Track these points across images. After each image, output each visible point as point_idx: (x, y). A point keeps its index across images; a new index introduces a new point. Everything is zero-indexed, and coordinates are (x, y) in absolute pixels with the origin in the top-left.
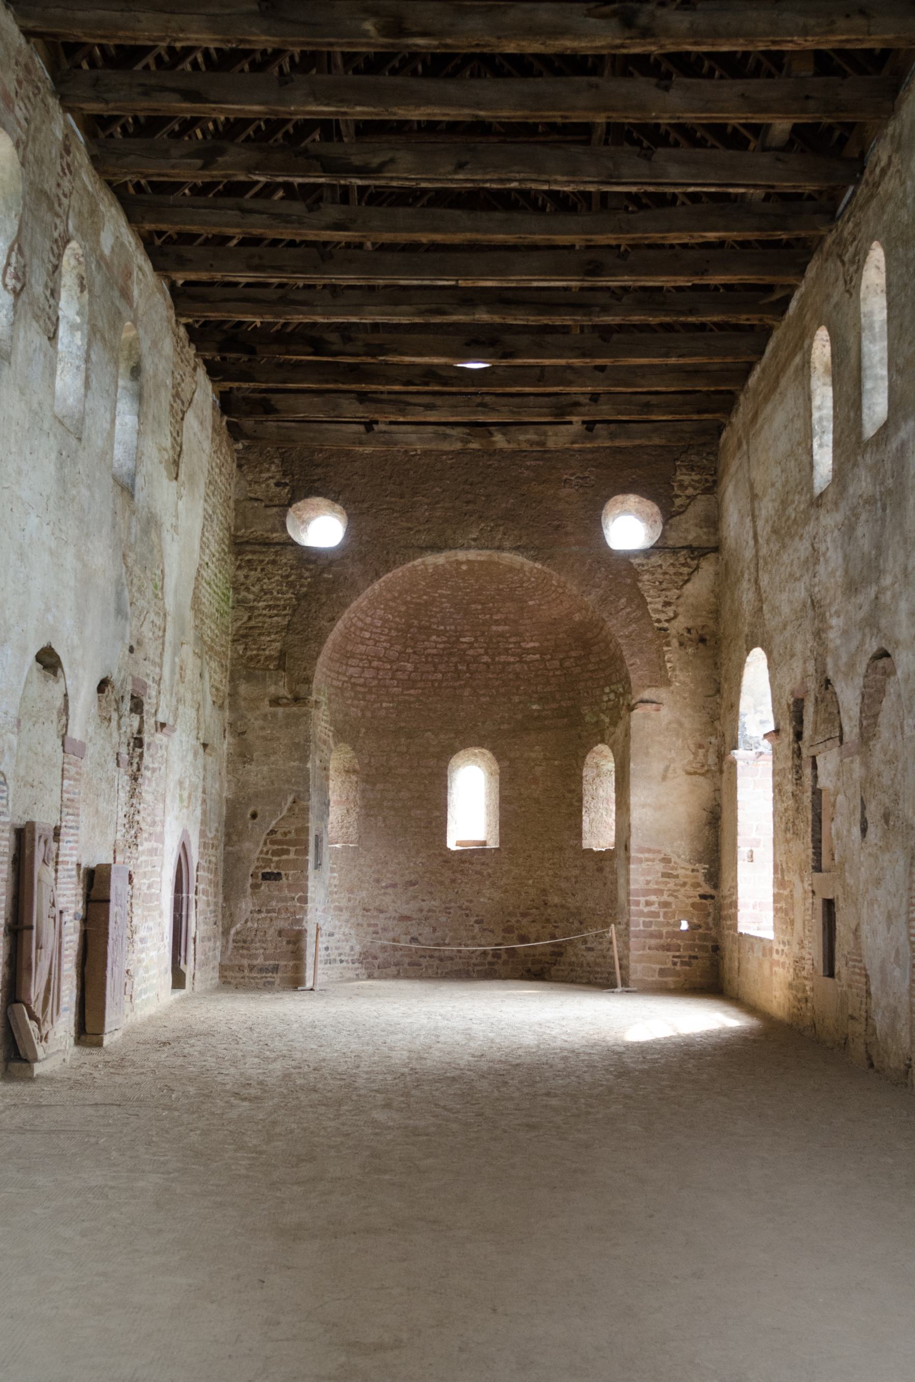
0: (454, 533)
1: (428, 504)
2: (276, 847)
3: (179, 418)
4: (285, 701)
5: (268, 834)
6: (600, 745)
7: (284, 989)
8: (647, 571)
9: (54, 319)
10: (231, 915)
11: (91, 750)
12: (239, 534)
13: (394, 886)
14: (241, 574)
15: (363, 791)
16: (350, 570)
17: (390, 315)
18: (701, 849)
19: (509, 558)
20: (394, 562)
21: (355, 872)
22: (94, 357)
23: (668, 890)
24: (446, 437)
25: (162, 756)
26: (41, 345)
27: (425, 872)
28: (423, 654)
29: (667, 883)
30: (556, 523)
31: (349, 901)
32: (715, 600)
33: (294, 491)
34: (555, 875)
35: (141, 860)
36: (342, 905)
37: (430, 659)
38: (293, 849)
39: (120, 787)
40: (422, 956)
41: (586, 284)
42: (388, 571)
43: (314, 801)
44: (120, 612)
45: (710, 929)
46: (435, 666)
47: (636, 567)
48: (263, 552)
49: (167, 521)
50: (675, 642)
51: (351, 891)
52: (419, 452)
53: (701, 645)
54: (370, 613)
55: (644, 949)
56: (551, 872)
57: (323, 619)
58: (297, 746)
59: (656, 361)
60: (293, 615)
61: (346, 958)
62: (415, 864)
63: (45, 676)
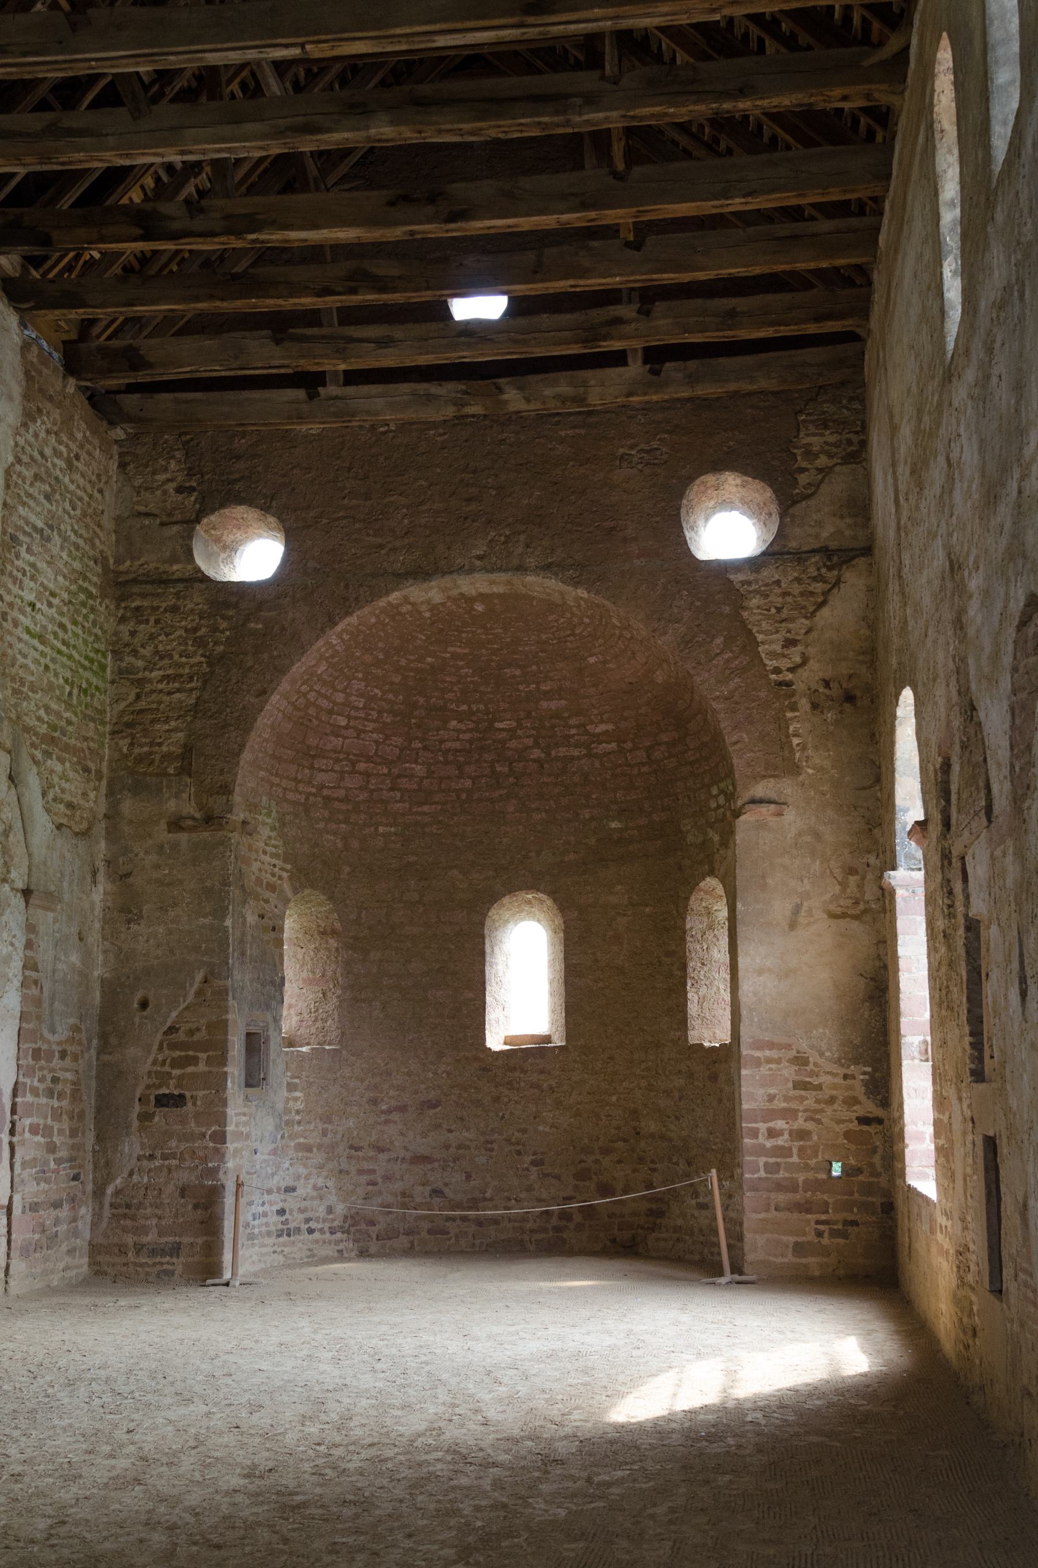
0: (449, 548)
2: (178, 1053)
4: (190, 823)
5: (165, 1033)
6: (708, 879)
7: (188, 1283)
8: (757, 592)
10: (107, 1164)
12: (122, 568)
13: (402, 1109)
14: (125, 629)
16: (290, 616)
18: (857, 1041)
20: (356, 599)
23: (805, 1111)
27: (452, 1087)
29: (802, 1099)
30: (608, 524)
31: (324, 1133)
32: (868, 633)
36: (311, 1141)
37: (451, 758)
38: (203, 1056)
42: (348, 614)
45: (879, 1175)
50: (804, 704)
51: (327, 1119)
53: (847, 706)
55: (767, 1211)
56: (644, 1083)
57: (248, 692)
60: (203, 689)
61: (320, 1226)
62: (435, 1073)
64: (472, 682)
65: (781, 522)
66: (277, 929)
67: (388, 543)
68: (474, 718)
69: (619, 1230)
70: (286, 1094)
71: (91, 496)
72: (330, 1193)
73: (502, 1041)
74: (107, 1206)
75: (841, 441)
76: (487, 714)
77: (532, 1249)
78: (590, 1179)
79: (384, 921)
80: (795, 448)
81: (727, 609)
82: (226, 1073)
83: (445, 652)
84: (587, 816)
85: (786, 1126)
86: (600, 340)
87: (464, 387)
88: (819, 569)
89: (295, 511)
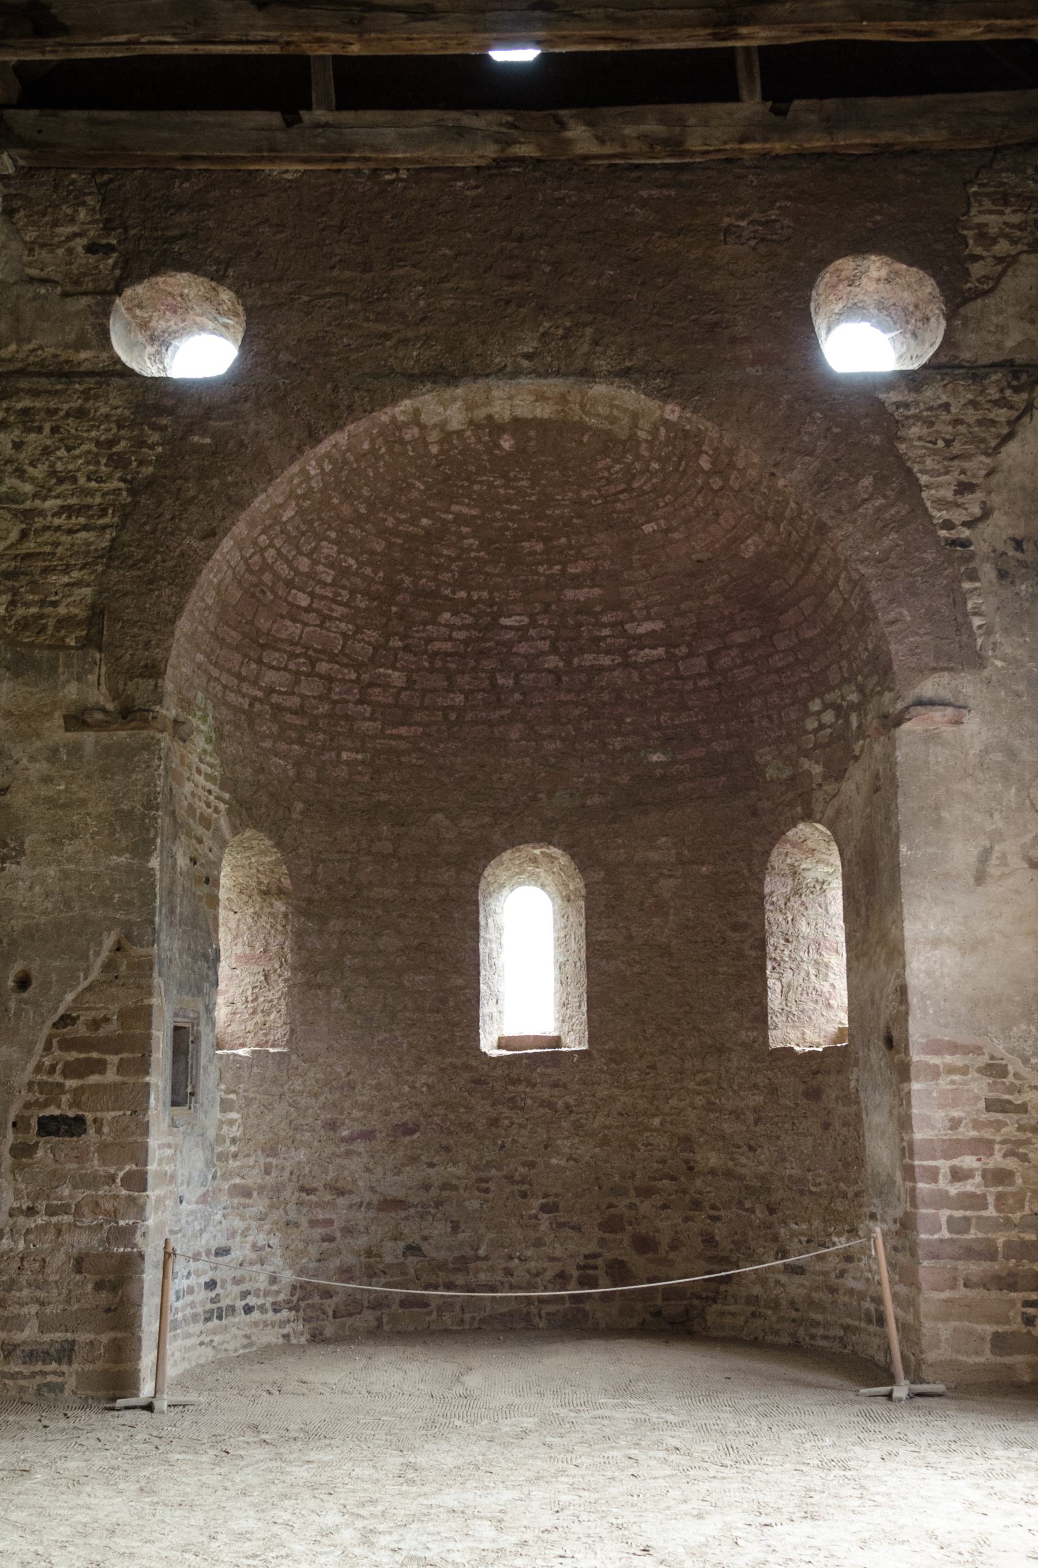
0: (484, 342)
1: (424, 284)
2: (73, 1055)
4: (99, 716)
6: (801, 826)
7: (85, 1404)
8: (917, 418)
13: (368, 1135)
15: (299, 935)
16: (252, 426)
20: (349, 407)
21: (281, 1108)
23: (1004, 1142)
27: (435, 1105)
28: (425, 652)
29: (998, 1125)
30: (710, 318)
33: (127, 261)
34: (710, 1106)
36: (249, 1182)
37: (439, 664)
38: (113, 1059)
46: (450, 677)
47: (891, 409)
48: (57, 392)
50: (988, 572)
51: (272, 1151)
54: (306, 549)
55: (953, 1287)
56: (700, 1100)
57: (189, 532)
58: (126, 818)
60: (121, 526)
61: (260, 1301)
62: (413, 1087)
64: (476, 559)
65: (948, 325)
66: (211, 881)
67: (398, 331)
68: (474, 611)
69: (664, 1300)
70: (219, 1116)
72: (274, 1254)
73: (495, 1044)
75: (1026, 222)
76: (491, 606)
77: (541, 1325)
78: (623, 1229)
79: (348, 879)
80: (964, 228)
81: (877, 440)
82: (148, 1085)
83: (448, 511)
84: (618, 747)
85: (976, 1165)
86: (740, 24)
87: (510, 119)
88: (1002, 391)
89: (262, 282)
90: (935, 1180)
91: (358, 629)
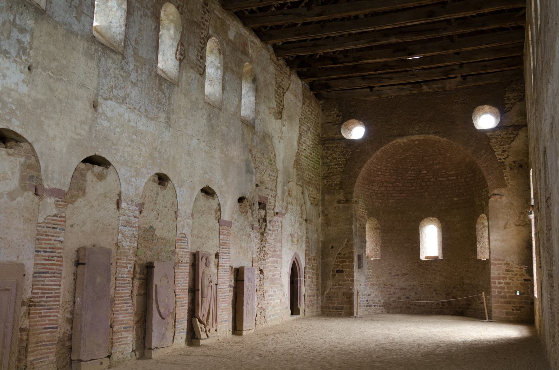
2: (341, 260)
3: (281, 96)
4: (342, 201)
8: (494, 138)
9: (203, 67)
11: (236, 224)
12: (323, 136)
13: (398, 275)
14: (324, 152)
15: (382, 237)
16: (367, 148)
17: (355, 45)
19: (432, 137)
22: (226, 78)
24: (402, 89)
25: (278, 225)
26: (195, 77)
29: (508, 274)
31: (377, 281)
32: (526, 148)
35: (268, 264)
37: (409, 181)
38: (347, 260)
39: (254, 237)
40: (411, 305)
41: (429, 21)
42: (382, 147)
43: (356, 241)
44: (249, 171)
48: (332, 143)
49: (276, 135)
50: (508, 168)
52: (393, 97)
53: (520, 168)
55: (498, 303)
56: (465, 270)
59: (476, 48)
62: (407, 266)
63: (207, 198)
66: (364, 228)
71: (316, 120)
74: (325, 297)
90: (495, 284)
91: (391, 177)
